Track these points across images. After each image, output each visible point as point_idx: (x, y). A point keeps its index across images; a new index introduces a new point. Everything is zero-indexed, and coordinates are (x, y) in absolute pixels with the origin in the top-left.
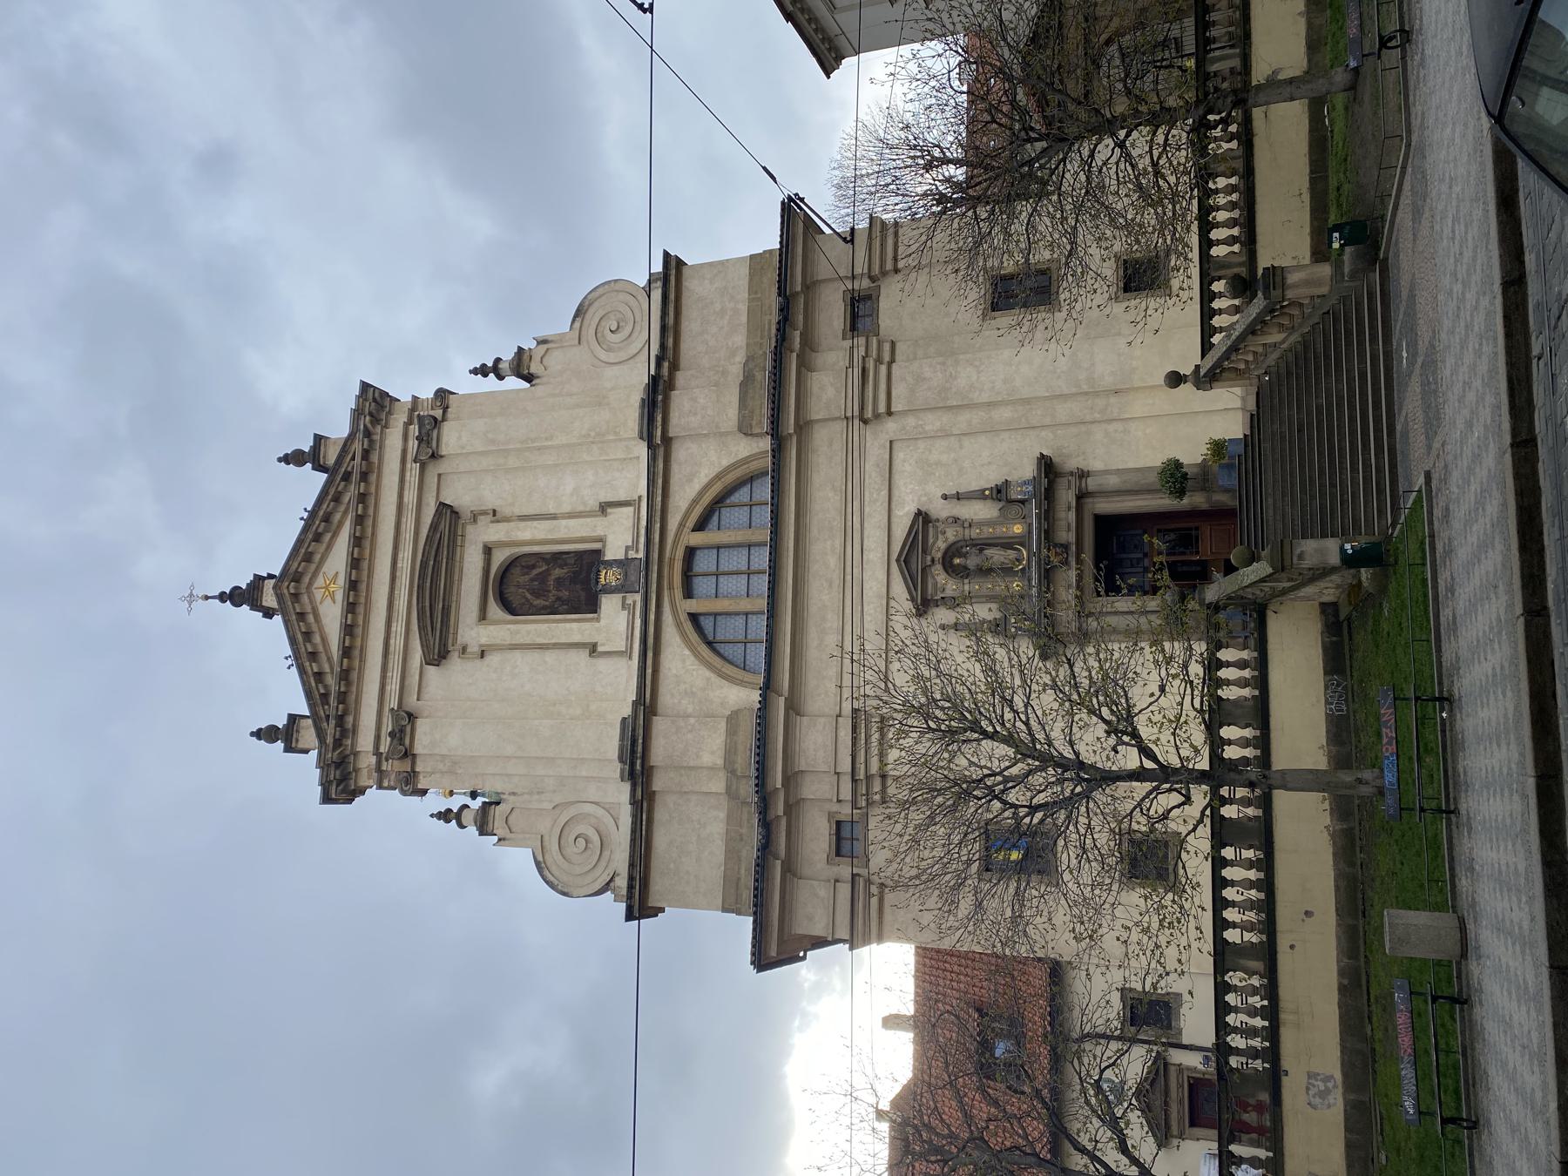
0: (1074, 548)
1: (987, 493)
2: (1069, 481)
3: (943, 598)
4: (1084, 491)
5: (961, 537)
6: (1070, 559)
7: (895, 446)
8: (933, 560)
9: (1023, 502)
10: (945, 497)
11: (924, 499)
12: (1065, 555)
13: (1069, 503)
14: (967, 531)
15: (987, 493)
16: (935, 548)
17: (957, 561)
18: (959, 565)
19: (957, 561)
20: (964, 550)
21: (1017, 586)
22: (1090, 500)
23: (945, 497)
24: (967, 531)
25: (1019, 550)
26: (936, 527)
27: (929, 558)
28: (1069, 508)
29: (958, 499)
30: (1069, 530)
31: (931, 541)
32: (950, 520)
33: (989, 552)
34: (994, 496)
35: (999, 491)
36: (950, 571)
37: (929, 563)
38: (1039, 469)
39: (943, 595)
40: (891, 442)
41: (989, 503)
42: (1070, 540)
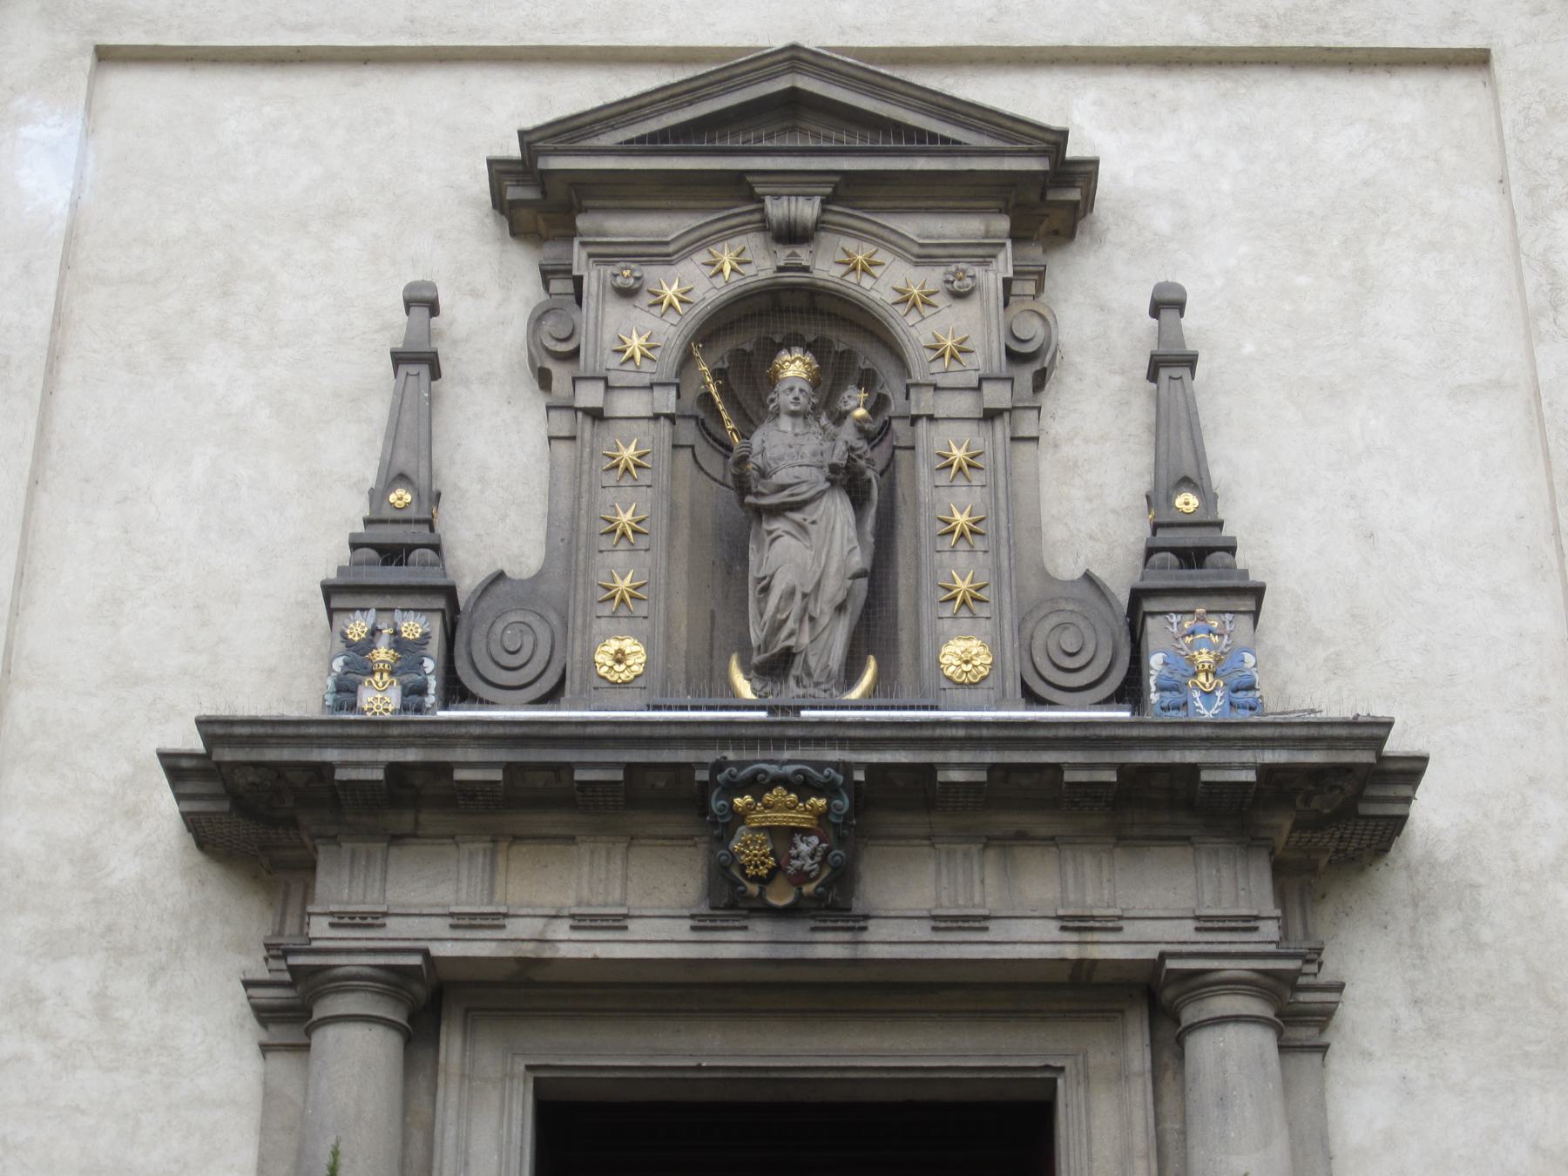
0: (829, 947)
1: (1187, 502)
2: (1248, 923)
3: (578, 282)
4: (1189, 1015)
5: (921, 365)
6: (761, 929)
7: (1458, 87)
8: (791, 235)
9: (1131, 690)
10: (1167, 304)
11: (1161, 220)
12: (780, 897)
13: (1111, 925)
14: (964, 404)
15: (1187, 502)
16: (861, 252)
17: (794, 367)
18: (773, 381)
19: (794, 367)
20: (856, 404)
21: (620, 657)
22: (1138, 1055)
23: (1167, 304)
24: (964, 404)
25: (851, 675)
26: (984, 253)
27: (807, 210)
28: (1076, 924)
29: (1156, 366)
30: (944, 922)
31: (912, 227)
32: (1030, 329)
33: (837, 511)
34: (1165, 537)
35: (1192, 557)
36: (746, 341)
37: (778, 209)
38: (1317, 733)
39: (591, 286)
40: (1477, 60)
41: (1136, 532)
42: (876, 930)
